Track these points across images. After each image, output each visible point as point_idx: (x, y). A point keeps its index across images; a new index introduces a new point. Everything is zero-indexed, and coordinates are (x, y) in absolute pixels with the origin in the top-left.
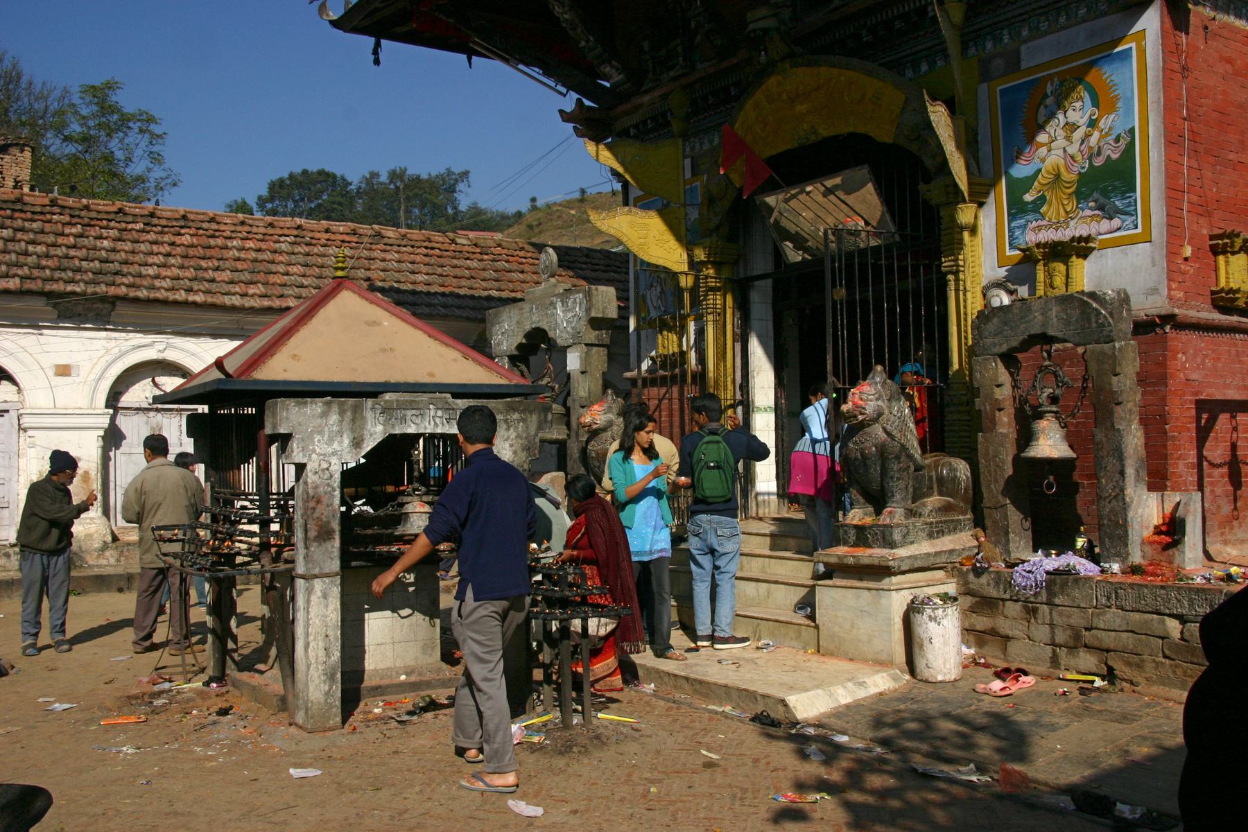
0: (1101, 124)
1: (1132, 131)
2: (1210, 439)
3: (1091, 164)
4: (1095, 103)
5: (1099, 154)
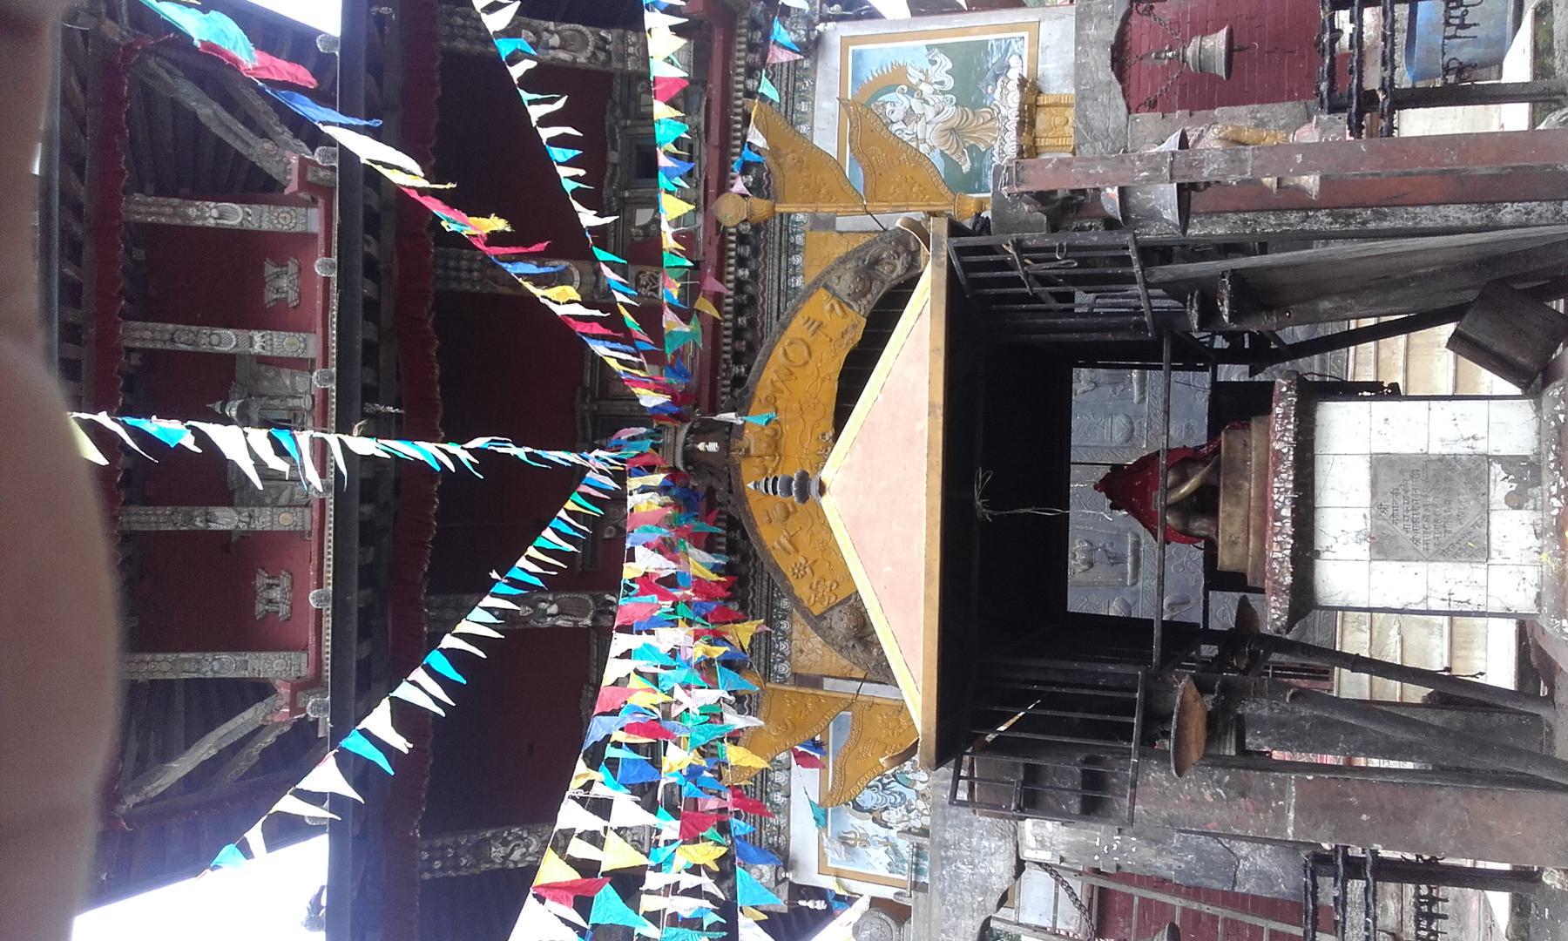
0: (914, 81)
1: (929, 47)
2: (1251, 107)
3: (949, 92)
4: (891, 89)
5: (942, 83)
